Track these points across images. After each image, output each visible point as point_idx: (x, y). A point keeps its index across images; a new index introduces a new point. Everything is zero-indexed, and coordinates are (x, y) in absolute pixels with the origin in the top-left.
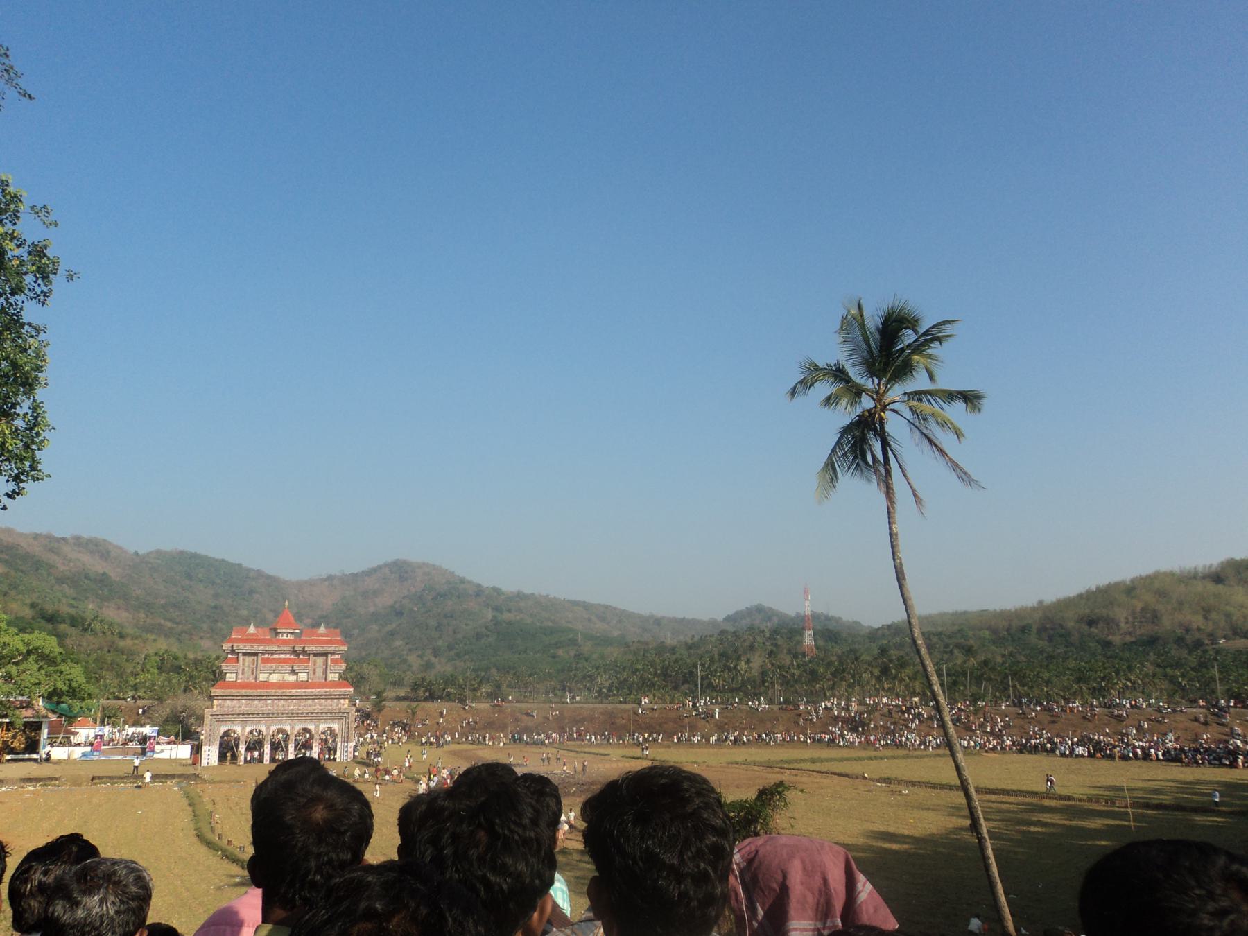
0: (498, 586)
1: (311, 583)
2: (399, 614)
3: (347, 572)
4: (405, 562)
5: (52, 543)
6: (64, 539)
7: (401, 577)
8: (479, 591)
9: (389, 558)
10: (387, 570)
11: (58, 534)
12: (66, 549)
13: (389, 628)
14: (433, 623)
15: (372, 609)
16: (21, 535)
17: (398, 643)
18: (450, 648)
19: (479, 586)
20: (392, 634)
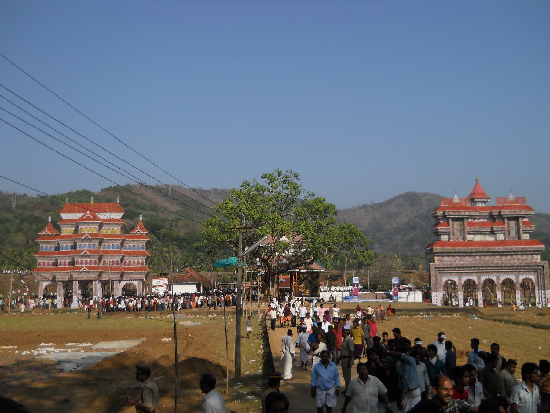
1: (353, 210)
2: (414, 228)
3: (376, 202)
4: (413, 193)
5: (202, 193)
6: (208, 191)
9: (403, 192)
10: (401, 199)
11: (205, 188)
12: (211, 197)
13: (408, 237)
15: (395, 226)
16: (185, 189)
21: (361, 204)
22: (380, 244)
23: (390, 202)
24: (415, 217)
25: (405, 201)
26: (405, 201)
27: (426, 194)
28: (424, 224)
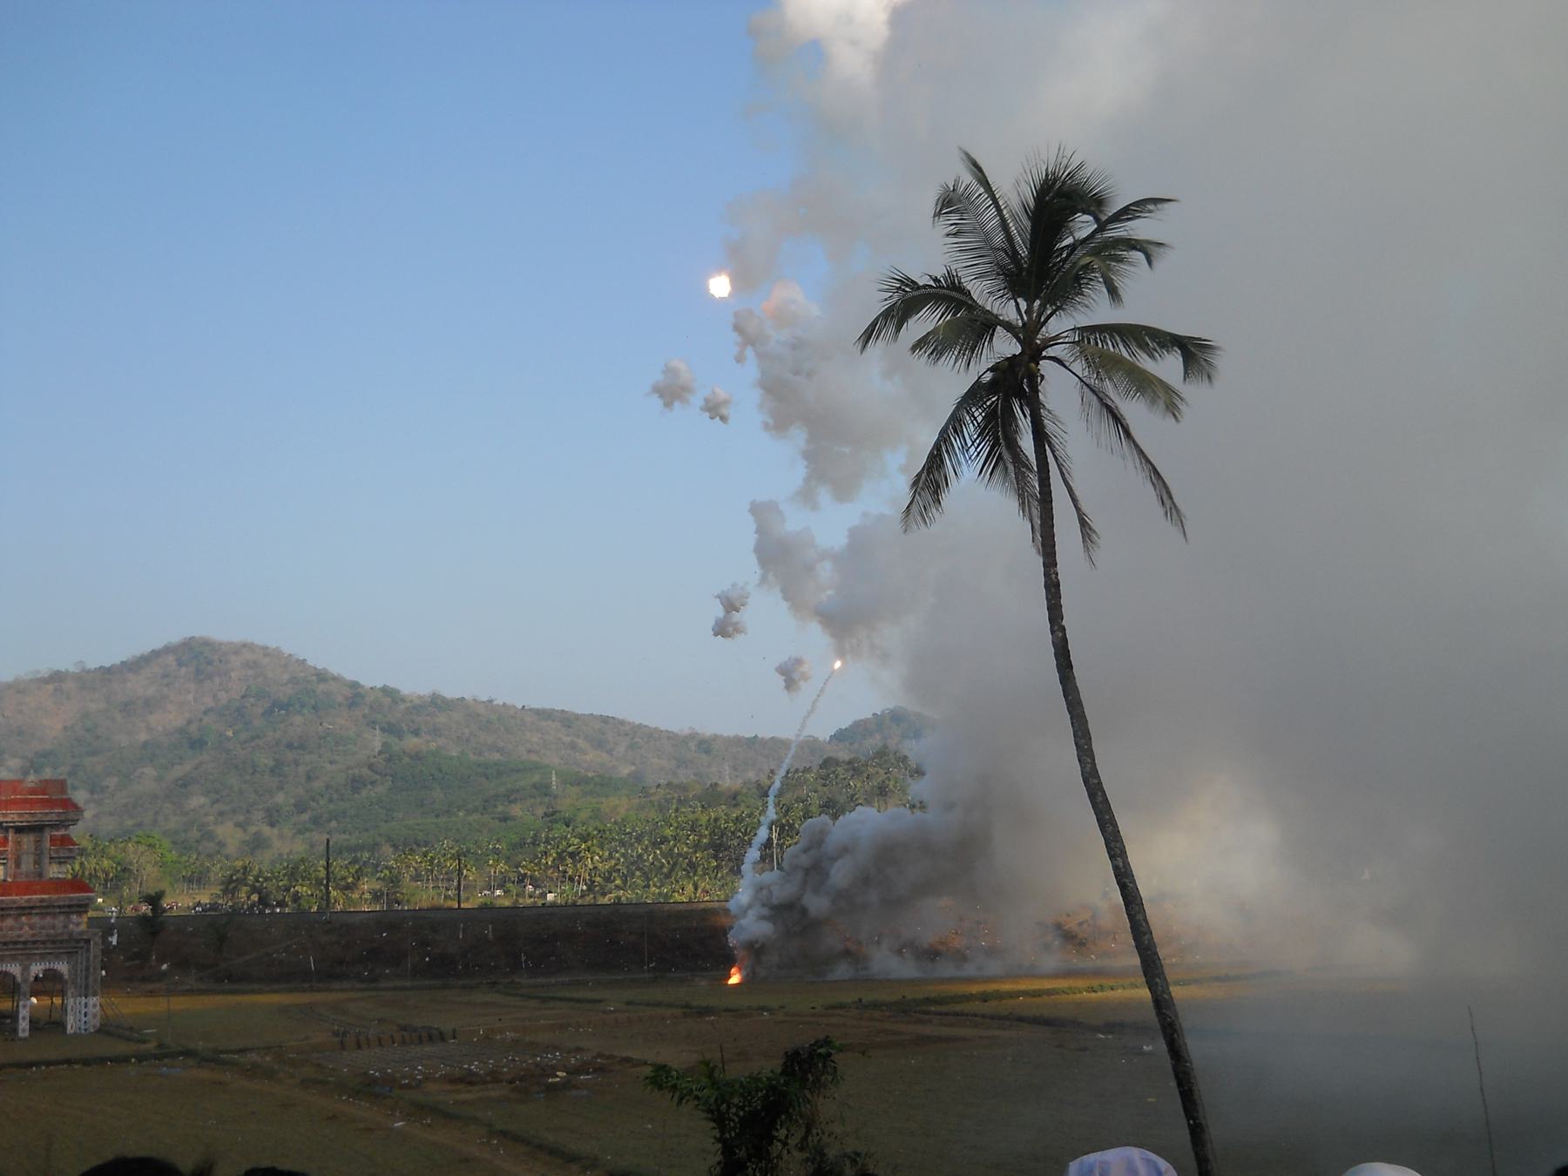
0: (392, 684)
2: (197, 744)
3: (92, 664)
4: (206, 643)
7: (198, 672)
8: (355, 694)
9: (175, 638)
10: (171, 659)
13: (178, 771)
14: (265, 760)
15: (143, 737)
17: (197, 801)
18: (300, 807)
19: (355, 685)
20: (185, 783)
21: (45, 667)
22: (92, 792)
23: (135, 665)
24: (205, 713)
25: (180, 664)
26: (180, 664)
27: (245, 645)
28: (230, 733)
